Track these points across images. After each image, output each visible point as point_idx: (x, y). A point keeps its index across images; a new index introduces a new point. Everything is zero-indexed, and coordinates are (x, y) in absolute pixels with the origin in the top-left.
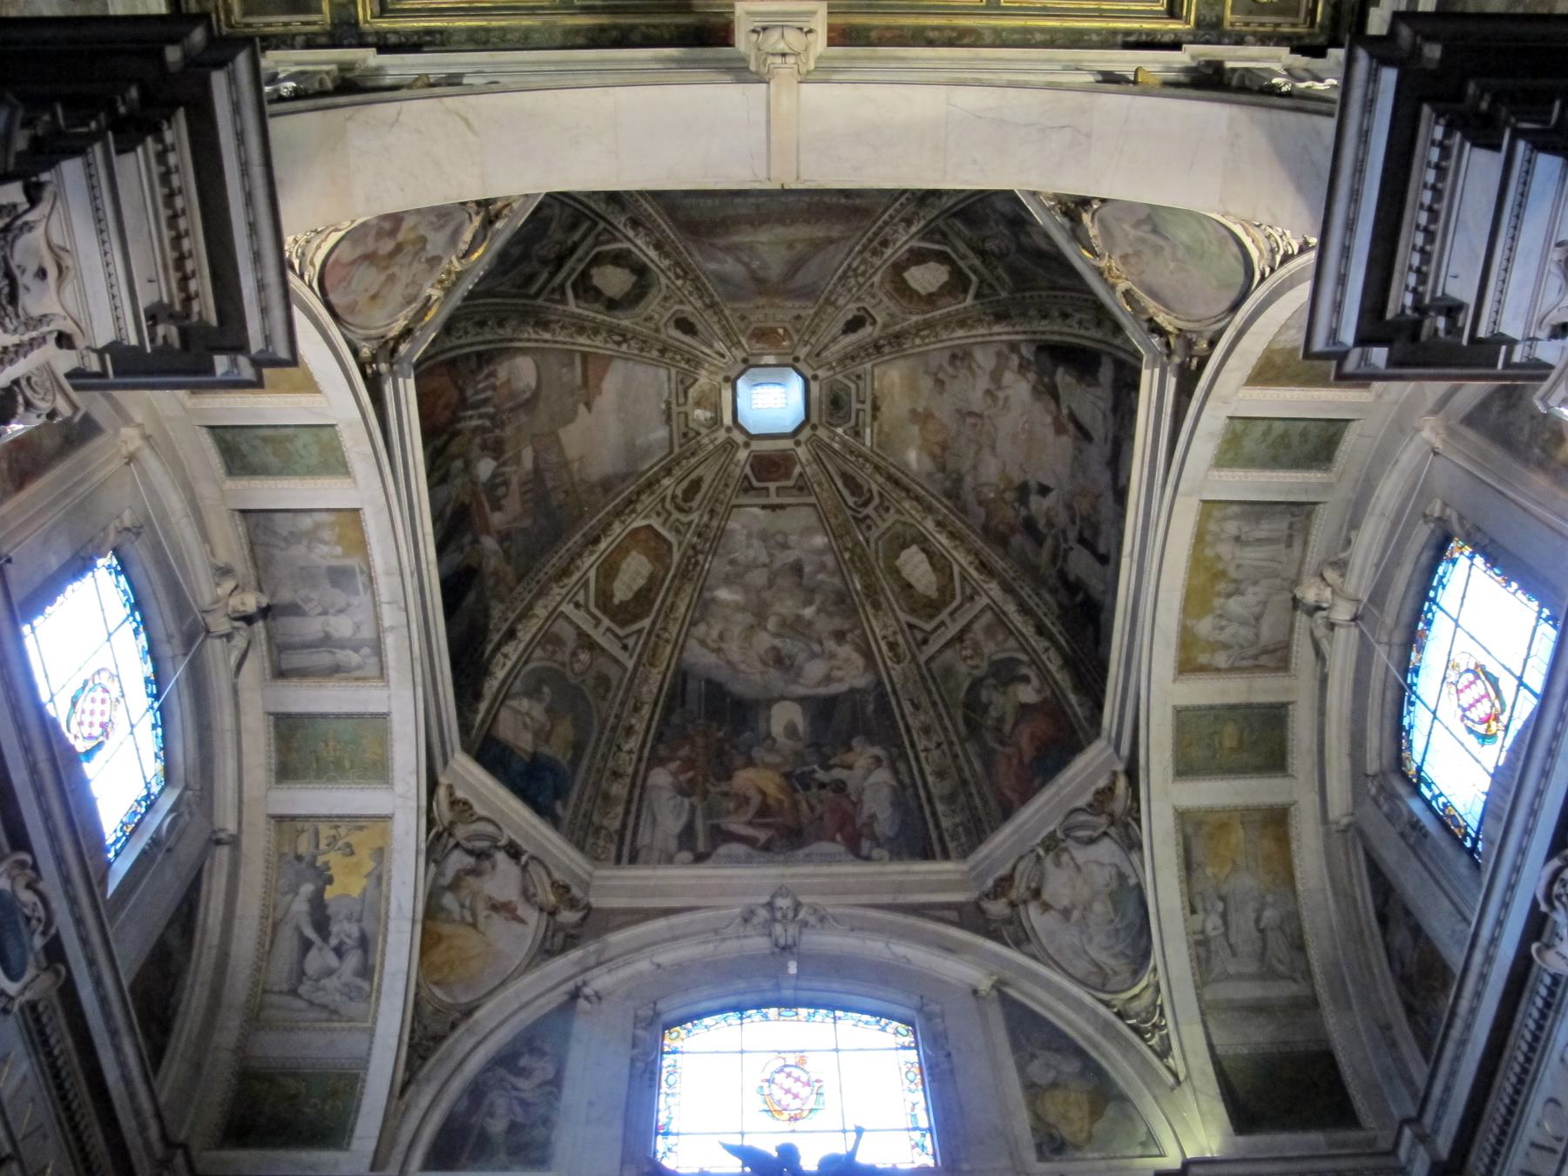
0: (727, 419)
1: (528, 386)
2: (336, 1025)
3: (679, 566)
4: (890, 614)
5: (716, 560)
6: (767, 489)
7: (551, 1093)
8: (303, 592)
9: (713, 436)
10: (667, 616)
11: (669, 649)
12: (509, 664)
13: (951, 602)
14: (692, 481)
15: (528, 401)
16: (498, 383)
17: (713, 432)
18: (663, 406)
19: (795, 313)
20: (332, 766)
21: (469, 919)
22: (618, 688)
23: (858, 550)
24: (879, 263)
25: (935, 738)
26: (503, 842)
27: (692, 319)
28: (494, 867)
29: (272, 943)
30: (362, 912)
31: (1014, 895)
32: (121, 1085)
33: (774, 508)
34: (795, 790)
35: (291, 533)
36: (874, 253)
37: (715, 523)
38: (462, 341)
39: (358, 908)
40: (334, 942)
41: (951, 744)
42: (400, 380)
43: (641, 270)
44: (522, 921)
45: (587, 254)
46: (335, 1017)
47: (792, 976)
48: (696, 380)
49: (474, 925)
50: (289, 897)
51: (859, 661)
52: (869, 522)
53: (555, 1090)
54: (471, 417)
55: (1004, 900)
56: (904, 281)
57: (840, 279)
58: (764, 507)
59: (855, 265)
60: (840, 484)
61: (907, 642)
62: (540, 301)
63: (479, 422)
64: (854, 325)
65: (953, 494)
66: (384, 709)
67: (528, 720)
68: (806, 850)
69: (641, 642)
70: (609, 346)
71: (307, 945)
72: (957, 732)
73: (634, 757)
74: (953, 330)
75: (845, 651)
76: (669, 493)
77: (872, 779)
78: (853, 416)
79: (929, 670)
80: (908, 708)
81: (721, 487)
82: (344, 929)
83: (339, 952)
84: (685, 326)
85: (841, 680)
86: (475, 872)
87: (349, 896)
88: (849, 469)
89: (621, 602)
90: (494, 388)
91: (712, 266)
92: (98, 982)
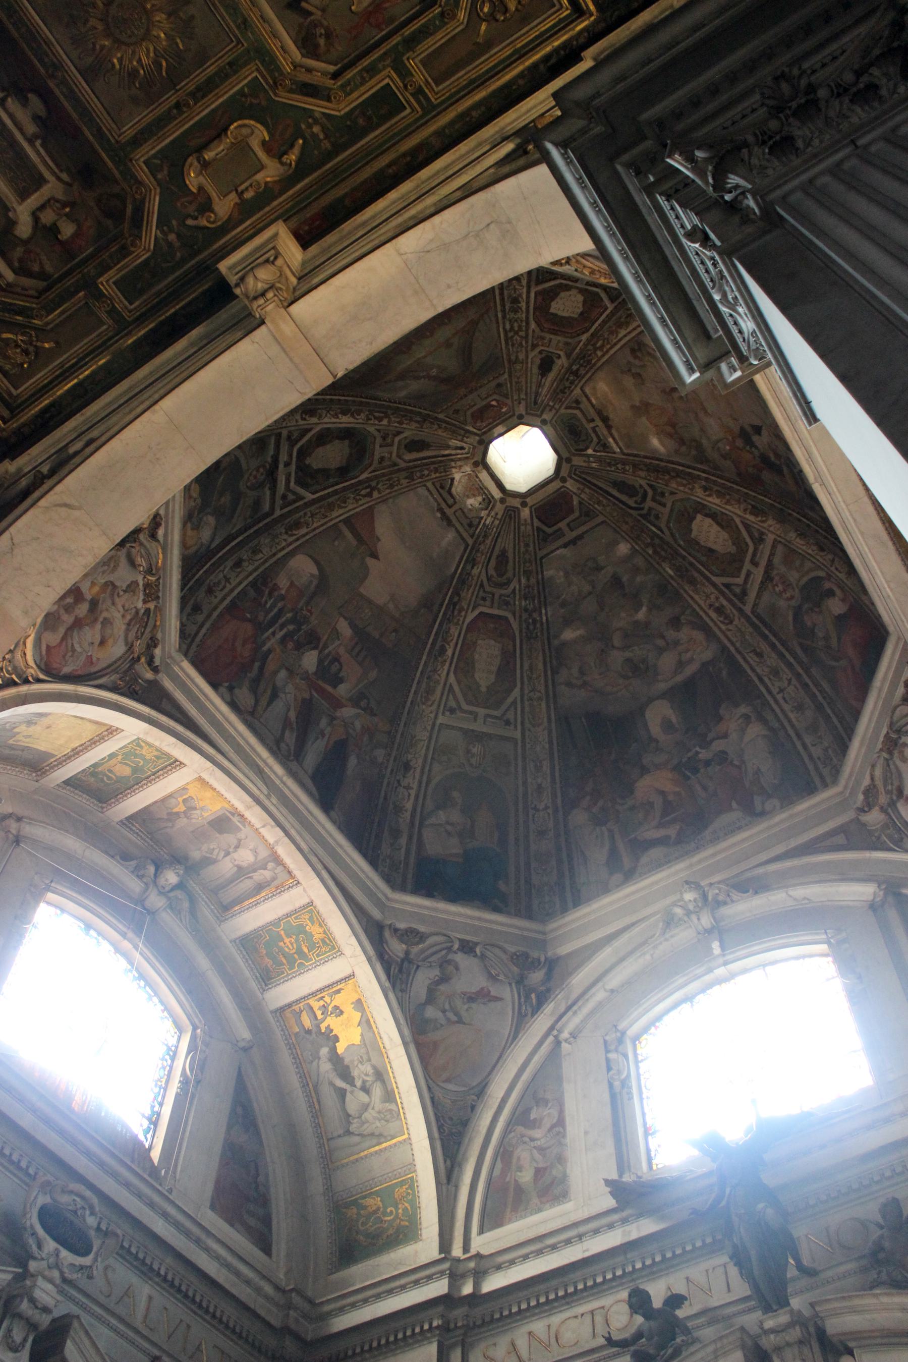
0: (497, 494)
1: (312, 575)
2: (384, 1145)
3: (521, 631)
4: (707, 584)
5: (548, 609)
6: (560, 529)
7: (558, 1133)
8: (205, 848)
9: (493, 514)
10: (530, 678)
11: (543, 704)
12: (413, 793)
13: (747, 550)
14: (498, 557)
15: (317, 587)
16: (283, 592)
17: (492, 509)
18: (439, 515)
19: (493, 384)
21: (455, 1018)
22: (516, 759)
23: (657, 541)
24: (524, 316)
25: (785, 676)
26: (456, 946)
27: (416, 439)
28: (457, 969)
29: (319, 1102)
30: (368, 1053)
31: (883, 799)
32: (224, 1271)
33: (573, 542)
34: (689, 778)
35: (169, 814)
36: (516, 311)
37: (533, 581)
38: (226, 590)
39: (363, 1051)
40: (359, 1083)
41: (798, 676)
42: (176, 669)
43: (347, 434)
44: (497, 999)
45: (291, 456)
46: (382, 1140)
47: (719, 956)
48: (453, 479)
49: (460, 1021)
50: (315, 1063)
51: (699, 636)
52: (653, 512)
53: (561, 1130)
54: (274, 634)
55: (877, 808)
56: (556, 315)
57: (507, 343)
58: (565, 546)
59: (508, 327)
60: (615, 493)
61: (730, 601)
62: (278, 513)
63: (285, 630)
64: (546, 365)
65: (701, 457)
66: (306, 900)
67: (449, 828)
68: (710, 829)
69: (519, 712)
70: (361, 502)
71: (342, 1093)
72: (800, 663)
73: (550, 811)
74: (617, 333)
75: (685, 633)
76: (484, 577)
77: (747, 738)
78: (593, 435)
79: (758, 617)
80: (752, 659)
81: (522, 550)
82: (361, 1071)
83: (366, 1089)
84: (415, 445)
85: (691, 660)
86: (444, 979)
88: (620, 477)
89: (488, 687)
90: (282, 598)
91: (403, 394)
92: (165, 1215)
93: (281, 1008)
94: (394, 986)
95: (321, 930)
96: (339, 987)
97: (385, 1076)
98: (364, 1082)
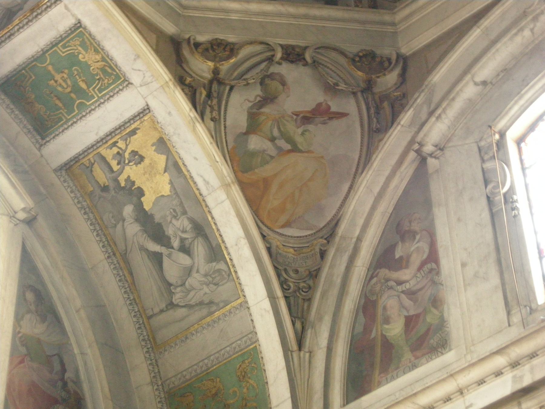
20: (73, 95)
26: (279, 55)
28: (283, 83)
30: (181, 204)
40: (176, 244)
49: (295, 149)
50: (119, 226)
71: (157, 259)
83: (185, 249)
87: (163, 196)
93: (66, 164)
94: (202, 116)
95: (98, 57)
96: (133, 127)
97: (207, 231)
98: (182, 240)
